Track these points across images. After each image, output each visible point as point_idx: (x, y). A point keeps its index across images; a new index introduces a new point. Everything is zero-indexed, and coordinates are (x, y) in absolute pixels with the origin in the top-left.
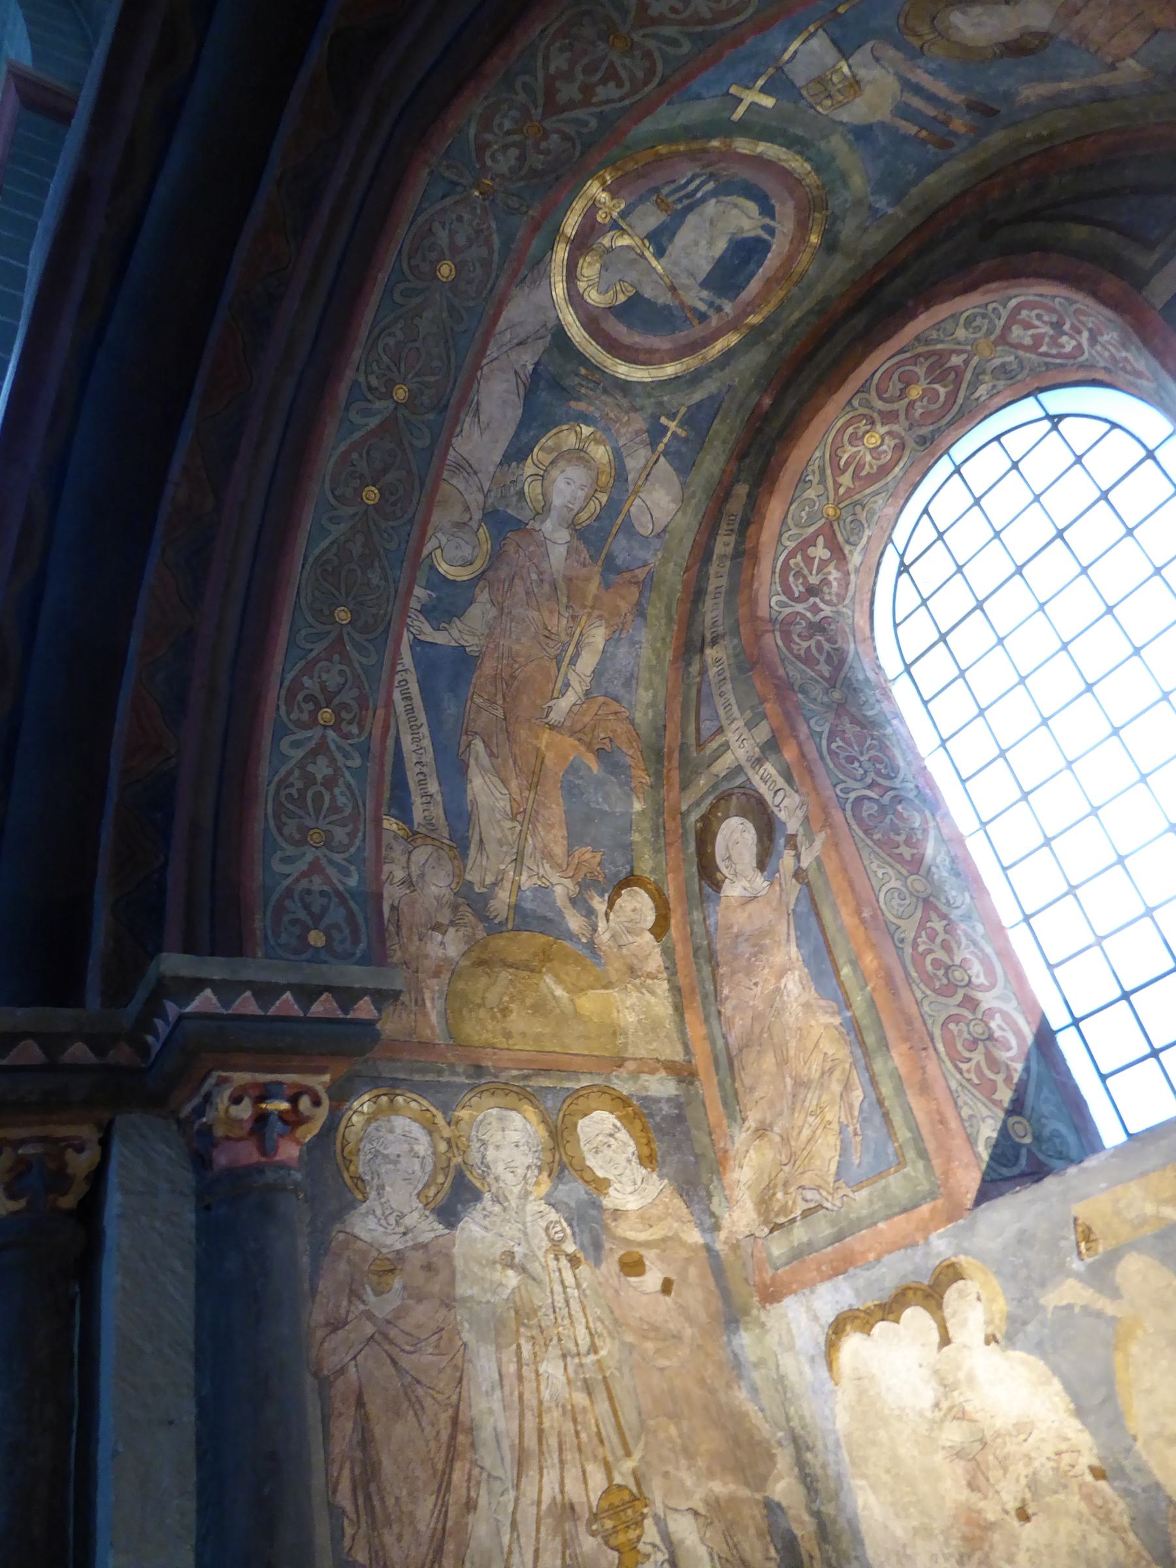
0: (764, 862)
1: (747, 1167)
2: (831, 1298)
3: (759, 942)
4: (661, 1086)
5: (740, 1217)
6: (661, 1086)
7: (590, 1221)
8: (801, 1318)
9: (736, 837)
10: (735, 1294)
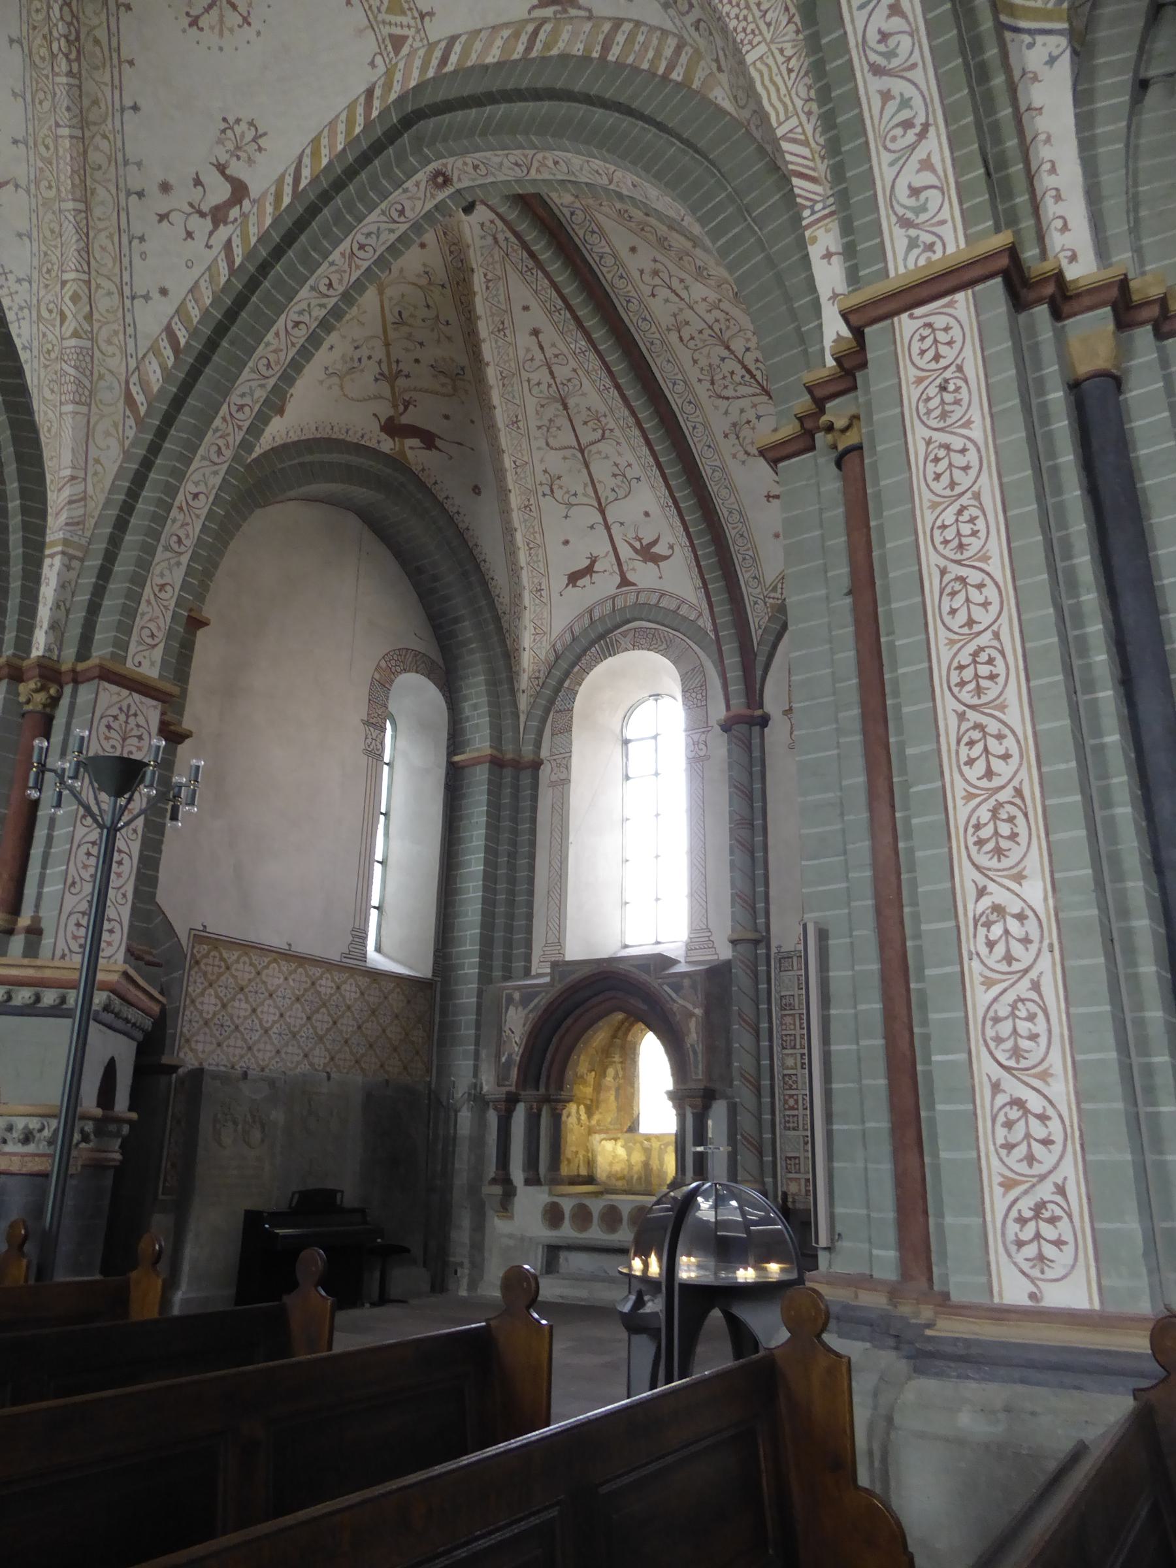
0: (614, 1079)
1: (596, 1117)
2: (603, 1136)
3: (609, 1089)
4: (589, 1102)
5: (594, 1122)
6: (589, 1102)
7: (579, 1119)
8: (597, 1137)
9: (611, 1072)
10: (591, 1131)
